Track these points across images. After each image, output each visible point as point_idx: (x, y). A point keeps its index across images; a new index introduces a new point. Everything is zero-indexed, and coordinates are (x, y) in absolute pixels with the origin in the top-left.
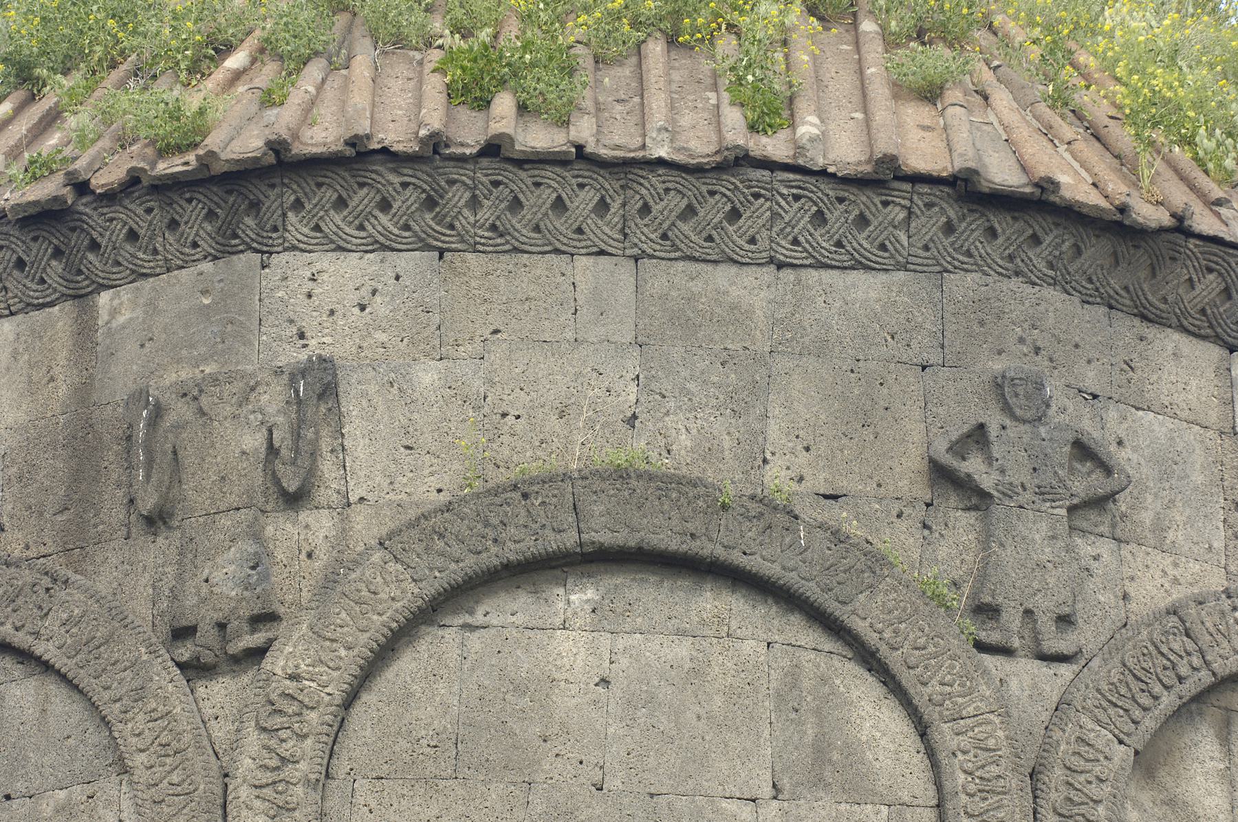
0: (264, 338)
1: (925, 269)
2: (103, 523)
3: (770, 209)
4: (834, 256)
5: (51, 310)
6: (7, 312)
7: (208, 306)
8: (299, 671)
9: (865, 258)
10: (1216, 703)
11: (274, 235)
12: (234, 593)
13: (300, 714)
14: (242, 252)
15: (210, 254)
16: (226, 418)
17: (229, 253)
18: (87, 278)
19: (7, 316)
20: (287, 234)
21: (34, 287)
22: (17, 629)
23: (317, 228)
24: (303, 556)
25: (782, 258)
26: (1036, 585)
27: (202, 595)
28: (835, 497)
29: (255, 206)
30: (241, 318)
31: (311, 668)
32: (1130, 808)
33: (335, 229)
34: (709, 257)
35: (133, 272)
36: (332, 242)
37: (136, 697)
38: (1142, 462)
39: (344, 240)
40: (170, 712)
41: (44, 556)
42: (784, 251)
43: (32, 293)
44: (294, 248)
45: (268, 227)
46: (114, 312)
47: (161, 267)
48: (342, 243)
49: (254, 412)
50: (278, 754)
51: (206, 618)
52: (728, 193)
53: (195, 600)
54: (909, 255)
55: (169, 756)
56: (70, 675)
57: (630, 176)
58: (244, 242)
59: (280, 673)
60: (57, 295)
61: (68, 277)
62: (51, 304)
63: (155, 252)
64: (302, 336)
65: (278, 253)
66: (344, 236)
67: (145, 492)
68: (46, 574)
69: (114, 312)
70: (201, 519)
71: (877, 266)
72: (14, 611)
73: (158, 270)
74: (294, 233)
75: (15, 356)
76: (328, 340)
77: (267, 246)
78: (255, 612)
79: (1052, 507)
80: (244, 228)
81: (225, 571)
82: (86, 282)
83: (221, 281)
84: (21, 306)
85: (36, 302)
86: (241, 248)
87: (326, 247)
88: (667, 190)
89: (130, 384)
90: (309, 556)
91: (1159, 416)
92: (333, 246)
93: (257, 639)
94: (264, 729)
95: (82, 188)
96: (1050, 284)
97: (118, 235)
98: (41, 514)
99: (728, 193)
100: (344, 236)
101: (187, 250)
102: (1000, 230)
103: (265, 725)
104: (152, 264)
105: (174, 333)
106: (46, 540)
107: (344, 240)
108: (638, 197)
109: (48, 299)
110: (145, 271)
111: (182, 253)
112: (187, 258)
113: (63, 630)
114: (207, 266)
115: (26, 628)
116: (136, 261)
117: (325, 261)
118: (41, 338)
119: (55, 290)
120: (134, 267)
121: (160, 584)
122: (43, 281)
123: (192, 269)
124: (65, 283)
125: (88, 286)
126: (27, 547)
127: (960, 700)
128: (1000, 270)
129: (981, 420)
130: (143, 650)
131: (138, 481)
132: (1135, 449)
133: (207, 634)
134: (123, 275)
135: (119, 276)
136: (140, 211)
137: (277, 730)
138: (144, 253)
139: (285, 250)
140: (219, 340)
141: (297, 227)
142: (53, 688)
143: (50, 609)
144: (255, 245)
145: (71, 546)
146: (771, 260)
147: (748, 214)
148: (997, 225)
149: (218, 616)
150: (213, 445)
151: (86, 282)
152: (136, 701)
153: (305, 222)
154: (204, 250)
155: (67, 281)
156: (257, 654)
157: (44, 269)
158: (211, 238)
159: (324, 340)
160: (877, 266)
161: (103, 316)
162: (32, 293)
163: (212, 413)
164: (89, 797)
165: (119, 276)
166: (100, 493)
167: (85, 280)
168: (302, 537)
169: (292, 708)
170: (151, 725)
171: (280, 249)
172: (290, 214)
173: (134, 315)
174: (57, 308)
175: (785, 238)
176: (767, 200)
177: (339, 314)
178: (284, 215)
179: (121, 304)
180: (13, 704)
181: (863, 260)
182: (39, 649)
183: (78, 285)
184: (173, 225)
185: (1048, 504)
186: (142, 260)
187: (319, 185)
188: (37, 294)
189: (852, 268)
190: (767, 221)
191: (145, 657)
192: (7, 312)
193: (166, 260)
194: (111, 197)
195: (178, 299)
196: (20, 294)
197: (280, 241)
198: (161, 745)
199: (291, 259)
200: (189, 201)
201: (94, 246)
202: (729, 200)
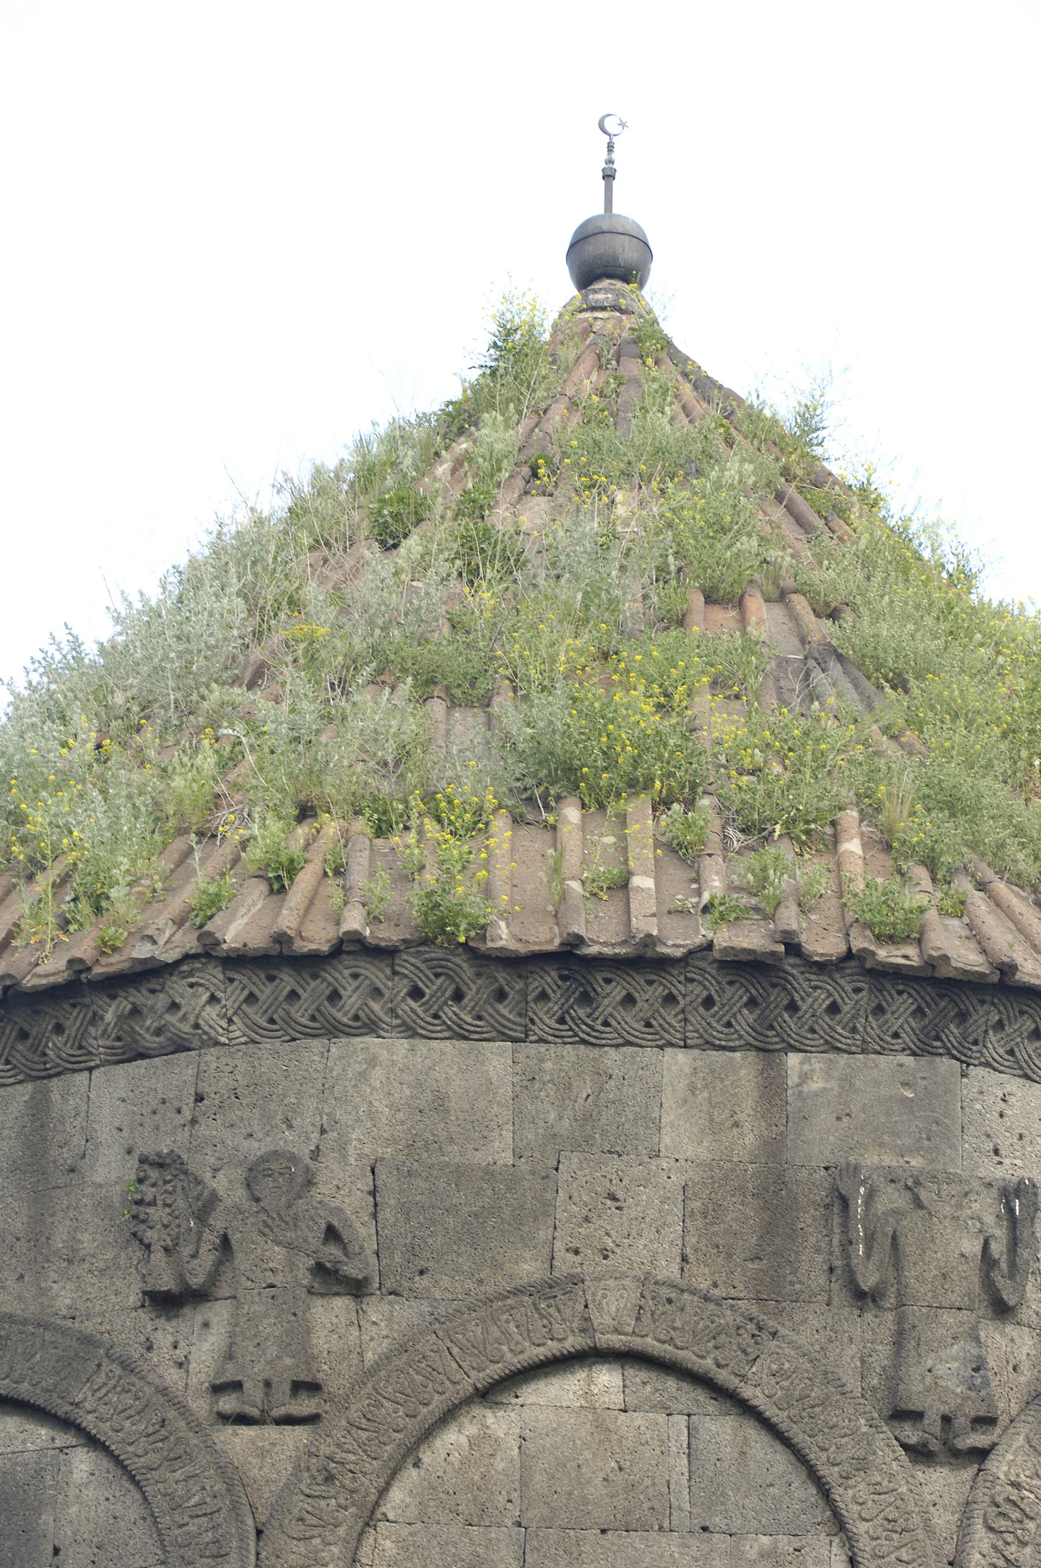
0: (967, 1146)
2: (801, 1283)
5: (731, 1054)
6: (682, 1043)
7: (911, 1100)
8: (1018, 1480)
11: (974, 1048)
12: (959, 1390)
13: (1020, 1522)
14: (941, 1055)
15: (910, 1049)
16: (945, 1217)
17: (929, 1052)
18: (778, 1035)
19: (681, 1047)
20: (985, 1051)
21: (719, 1028)
22: (719, 1366)
23: (1011, 1052)
24: (1010, 1368)
27: (927, 1383)
29: (963, 1017)
30: (947, 1121)
31: (1029, 1480)
33: (1026, 1057)
35: (827, 1042)
36: (1021, 1068)
37: (859, 1466)
39: (1031, 1069)
40: (896, 1490)
41: (733, 1299)
43: (715, 1033)
44: (988, 1065)
45: (971, 1039)
46: (805, 1077)
47: (857, 1046)
48: (1029, 1072)
49: (972, 1218)
50: (1004, 1556)
51: (934, 1410)
53: (921, 1388)
55: (896, 1532)
56: (783, 1427)
58: (945, 1047)
59: (1002, 1477)
60: (742, 1042)
61: (759, 1029)
62: (733, 1049)
63: (854, 1030)
64: (996, 1152)
65: (975, 1066)
66: (1033, 1067)
67: (866, 1268)
68: (751, 1320)
69: (805, 1077)
70: (923, 1309)
72: (716, 1348)
73: (854, 1049)
74: (992, 1051)
75: (692, 1089)
76: (1018, 1162)
77: (965, 1056)
78: (981, 1413)
80: (948, 1033)
81: (948, 1365)
82: (777, 1039)
83: (924, 1078)
84: (700, 1041)
85: (717, 1042)
86: (941, 1051)
87: (1015, 1072)
89: (827, 1153)
90: (1015, 1369)
92: (1021, 1072)
93: (979, 1439)
94: (991, 1529)
95: (793, 948)
97: (821, 1005)
98: (729, 1256)
100: (1033, 1067)
101: (889, 1039)
103: (993, 1525)
104: (849, 1041)
105: (873, 1116)
106: (736, 1283)
107: (1031, 1069)
109: (731, 1044)
110: (839, 1045)
111: (882, 1040)
112: (886, 1046)
113: (773, 1381)
114: (908, 1060)
115: (730, 1368)
116: (833, 1034)
117: (1014, 1085)
118: (722, 1080)
119: (741, 1037)
120: (829, 1039)
121: (871, 1359)
122: (729, 1025)
123: (891, 1058)
124: (754, 1034)
125: (776, 1043)
126: (715, 1285)
130: (863, 1421)
131: (858, 1255)
133: (933, 1423)
134: (816, 1043)
135: (812, 1043)
136: (848, 988)
137: (1002, 1532)
138: (843, 1029)
139: (980, 1064)
140: (924, 1136)
141: (995, 1046)
142: (753, 1432)
143: (758, 1357)
144: (955, 1052)
145: (765, 1297)
149: (945, 1409)
150: (933, 1239)
151: (777, 1039)
152: (858, 1470)
153: (1002, 1043)
154: (904, 1042)
155: (756, 1032)
156: (981, 1454)
157: (734, 1015)
158: (915, 1034)
159: (1016, 1162)
161: (793, 1079)
162: (715, 1033)
163: (932, 1209)
164: (795, 1550)
165: (812, 1043)
166: (797, 1253)
167: (774, 1036)
168: (1009, 1349)
169: (1015, 1515)
170: (876, 1497)
171: (976, 1062)
172: (991, 1032)
173: (829, 1086)
174: (738, 1054)
177: (1027, 1139)
178: (986, 1032)
179: (813, 1070)
180: (708, 1437)
182: (747, 1392)
183: (766, 1040)
184: (879, 1010)
186: (839, 1034)
187: (1022, 1013)
188: (721, 1035)
191: (865, 1429)
192: (682, 1043)
193: (864, 1041)
194: (822, 967)
195: (877, 1083)
196: (701, 1030)
197: (978, 1055)
198: (887, 1519)
199: (986, 1075)
200: (900, 993)
201: (792, 1007)
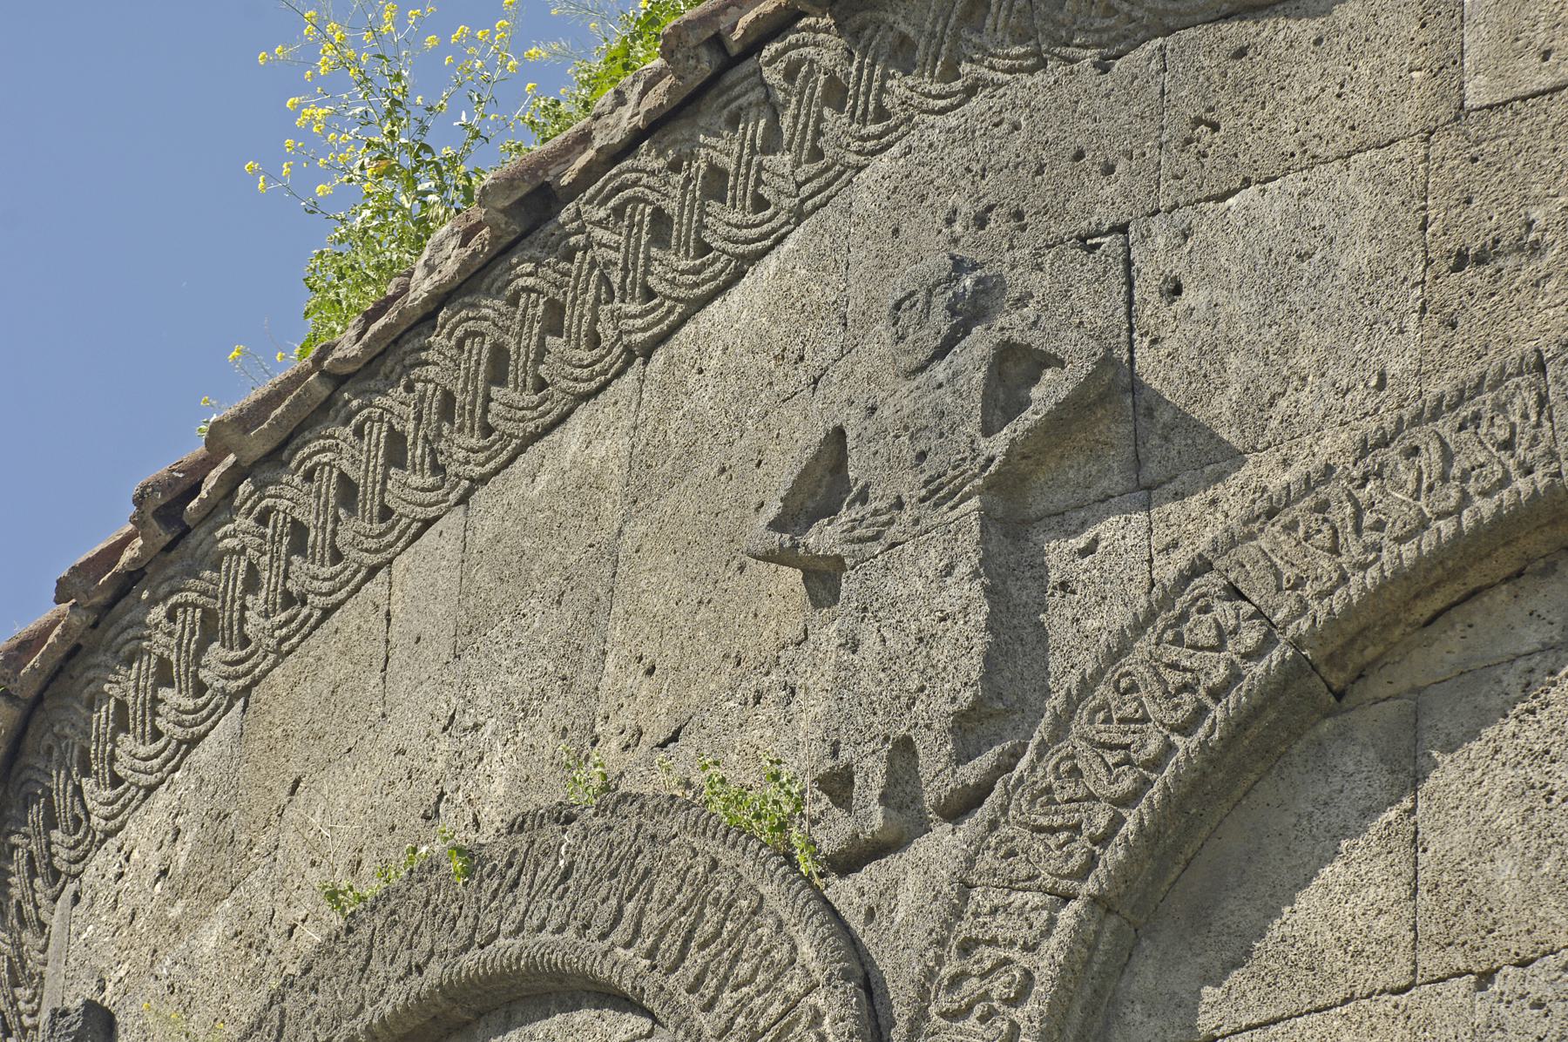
1: (827, 193)
3: (593, 264)
4: (707, 273)
9: (744, 243)
10: (1382, 692)
25: (639, 337)
26: (913, 685)
28: (674, 738)
32: (1138, 1017)
34: (548, 419)
38: (1220, 295)
42: (637, 320)
52: (530, 281)
54: (799, 186)
57: (407, 362)
71: (768, 243)
79: (952, 508)
88: (460, 345)
91: (1270, 185)
96: (1031, 71)
99: (530, 281)
102: (912, 33)
108: (431, 386)
127: (759, 1001)
128: (942, 103)
129: (838, 422)
132: (1209, 279)
146: (630, 354)
147: (570, 296)
148: (903, 27)
160: (768, 243)
175: (633, 299)
176: (585, 249)
181: (741, 249)
185: (945, 508)
189: (739, 275)
190: (598, 288)
202: (539, 293)
